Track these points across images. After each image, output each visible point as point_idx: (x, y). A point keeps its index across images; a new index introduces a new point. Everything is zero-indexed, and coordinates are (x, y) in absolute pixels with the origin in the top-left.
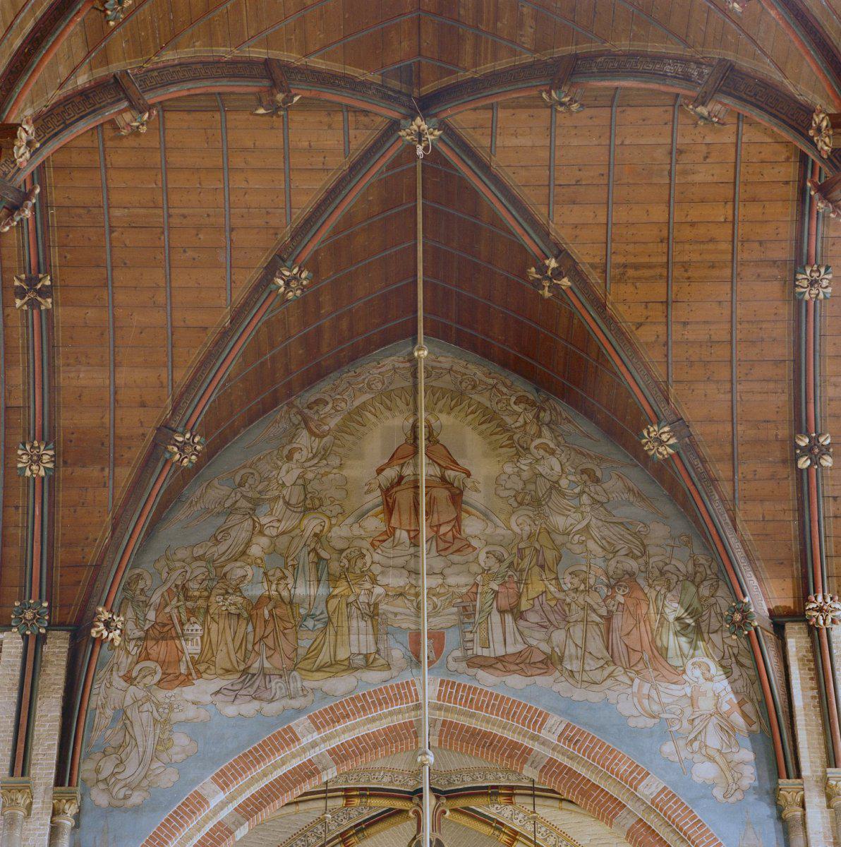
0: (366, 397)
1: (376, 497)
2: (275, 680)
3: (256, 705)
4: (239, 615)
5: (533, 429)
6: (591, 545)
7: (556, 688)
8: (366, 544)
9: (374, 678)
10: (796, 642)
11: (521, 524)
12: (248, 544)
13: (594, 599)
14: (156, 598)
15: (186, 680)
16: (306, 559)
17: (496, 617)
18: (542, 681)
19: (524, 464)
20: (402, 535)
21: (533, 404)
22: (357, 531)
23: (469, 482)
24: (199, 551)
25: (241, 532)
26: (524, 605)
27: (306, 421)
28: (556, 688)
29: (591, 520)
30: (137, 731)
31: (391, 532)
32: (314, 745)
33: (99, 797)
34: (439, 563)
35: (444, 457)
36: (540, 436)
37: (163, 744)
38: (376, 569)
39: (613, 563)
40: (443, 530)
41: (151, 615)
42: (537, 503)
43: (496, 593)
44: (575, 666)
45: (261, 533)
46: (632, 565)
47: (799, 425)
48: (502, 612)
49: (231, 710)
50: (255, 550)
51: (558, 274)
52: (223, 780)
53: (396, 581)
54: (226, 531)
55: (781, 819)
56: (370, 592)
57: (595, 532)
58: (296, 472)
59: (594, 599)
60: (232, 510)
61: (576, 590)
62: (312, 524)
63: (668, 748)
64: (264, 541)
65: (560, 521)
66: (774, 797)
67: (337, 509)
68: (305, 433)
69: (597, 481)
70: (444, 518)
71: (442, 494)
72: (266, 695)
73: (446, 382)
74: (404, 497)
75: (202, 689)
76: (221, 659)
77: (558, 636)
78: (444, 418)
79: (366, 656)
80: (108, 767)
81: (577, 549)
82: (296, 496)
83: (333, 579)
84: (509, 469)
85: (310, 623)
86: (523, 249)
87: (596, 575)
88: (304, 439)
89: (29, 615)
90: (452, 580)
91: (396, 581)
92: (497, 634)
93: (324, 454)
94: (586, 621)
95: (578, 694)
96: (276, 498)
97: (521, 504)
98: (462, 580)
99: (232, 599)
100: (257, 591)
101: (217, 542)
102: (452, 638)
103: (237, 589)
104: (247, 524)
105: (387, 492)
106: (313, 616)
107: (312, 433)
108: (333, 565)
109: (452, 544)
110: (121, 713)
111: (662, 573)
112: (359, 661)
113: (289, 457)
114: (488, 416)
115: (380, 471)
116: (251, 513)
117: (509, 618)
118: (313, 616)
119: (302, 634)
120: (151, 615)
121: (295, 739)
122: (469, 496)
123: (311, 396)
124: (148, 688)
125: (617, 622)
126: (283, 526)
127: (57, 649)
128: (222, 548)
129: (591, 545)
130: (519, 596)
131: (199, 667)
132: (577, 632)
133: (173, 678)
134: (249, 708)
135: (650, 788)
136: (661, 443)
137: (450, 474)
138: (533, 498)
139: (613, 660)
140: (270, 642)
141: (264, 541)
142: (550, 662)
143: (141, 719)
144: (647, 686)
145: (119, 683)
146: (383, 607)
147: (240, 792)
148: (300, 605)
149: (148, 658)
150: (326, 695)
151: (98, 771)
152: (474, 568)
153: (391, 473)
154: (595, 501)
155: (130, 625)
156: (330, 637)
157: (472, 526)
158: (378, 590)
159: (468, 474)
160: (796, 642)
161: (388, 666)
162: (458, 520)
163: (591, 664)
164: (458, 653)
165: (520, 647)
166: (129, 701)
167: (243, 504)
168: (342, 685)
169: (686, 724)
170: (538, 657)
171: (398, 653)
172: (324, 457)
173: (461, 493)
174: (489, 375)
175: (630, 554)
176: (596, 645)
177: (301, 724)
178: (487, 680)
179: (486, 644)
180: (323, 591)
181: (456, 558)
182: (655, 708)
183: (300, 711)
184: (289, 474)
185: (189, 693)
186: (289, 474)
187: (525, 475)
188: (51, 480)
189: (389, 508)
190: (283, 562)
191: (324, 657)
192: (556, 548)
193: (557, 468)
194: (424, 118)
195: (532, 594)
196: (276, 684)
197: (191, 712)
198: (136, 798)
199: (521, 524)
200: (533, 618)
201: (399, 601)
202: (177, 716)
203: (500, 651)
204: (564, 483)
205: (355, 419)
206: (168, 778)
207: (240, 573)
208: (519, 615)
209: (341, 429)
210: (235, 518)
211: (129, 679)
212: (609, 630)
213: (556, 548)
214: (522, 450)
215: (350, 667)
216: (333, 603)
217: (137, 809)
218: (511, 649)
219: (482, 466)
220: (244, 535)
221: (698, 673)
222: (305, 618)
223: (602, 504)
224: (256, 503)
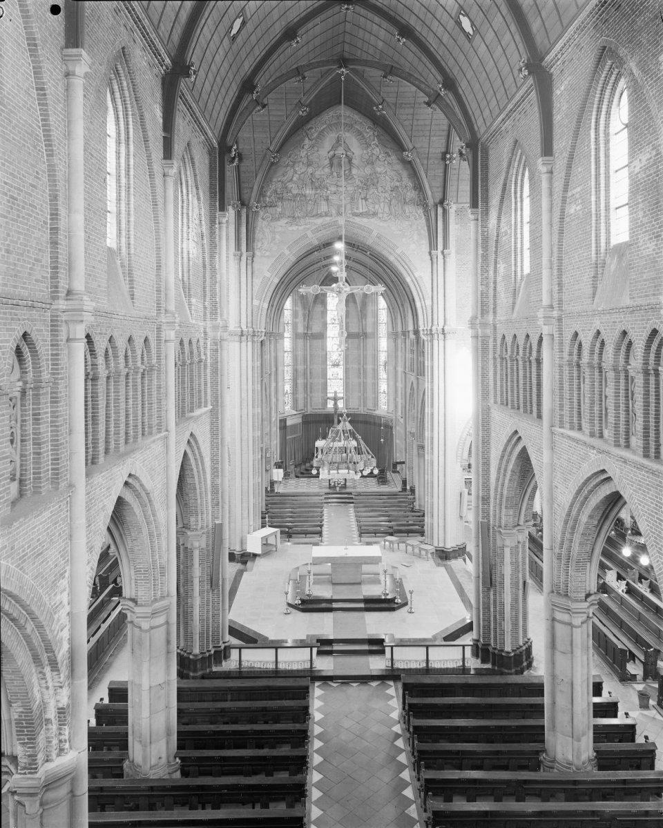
1: (327, 162)
9: (328, 219)
10: (440, 210)
11: (368, 170)
15: (278, 219)
16: (309, 181)
17: (360, 201)
18: (372, 220)
20: (335, 174)
22: (322, 173)
25: (290, 173)
29: (388, 170)
31: (332, 174)
33: (258, 253)
35: (347, 149)
37: (273, 239)
38: (328, 185)
41: (268, 199)
42: (372, 163)
46: (398, 184)
47: (447, 152)
49: (290, 229)
50: (295, 179)
51: (382, 109)
53: (333, 189)
55: (431, 259)
58: (305, 153)
59: (387, 195)
60: (288, 165)
62: (310, 170)
63: (404, 240)
64: (297, 176)
65: (379, 170)
66: (430, 253)
74: (335, 161)
75: (283, 222)
76: (287, 213)
77: (377, 207)
82: (305, 160)
83: (316, 188)
86: (372, 101)
87: (388, 188)
88: (307, 141)
91: (333, 189)
92: (360, 206)
93: (312, 147)
95: (381, 224)
100: (295, 192)
102: (349, 207)
105: (331, 159)
107: (309, 139)
108: (317, 184)
109: (349, 177)
114: (360, 133)
116: (293, 166)
122: (354, 161)
123: (309, 126)
127: (244, 211)
131: (281, 216)
132: (382, 205)
133: (274, 219)
134: (295, 228)
135: (398, 251)
137: (349, 153)
141: (297, 176)
142: (375, 214)
143: (267, 231)
146: (330, 197)
153: (332, 153)
154: (388, 163)
157: (354, 171)
160: (440, 210)
162: (350, 169)
167: (291, 163)
168: (319, 221)
170: (371, 213)
171: (334, 212)
176: (387, 209)
177: (309, 234)
178: (357, 220)
179: (357, 209)
184: (303, 153)
185: (279, 223)
189: (331, 165)
191: (314, 213)
194: (346, 67)
197: (280, 229)
198: (267, 254)
200: (370, 200)
203: (361, 211)
205: (321, 135)
208: (366, 199)
209: (318, 137)
210: (289, 168)
214: (368, 145)
215: (321, 216)
219: (356, 149)
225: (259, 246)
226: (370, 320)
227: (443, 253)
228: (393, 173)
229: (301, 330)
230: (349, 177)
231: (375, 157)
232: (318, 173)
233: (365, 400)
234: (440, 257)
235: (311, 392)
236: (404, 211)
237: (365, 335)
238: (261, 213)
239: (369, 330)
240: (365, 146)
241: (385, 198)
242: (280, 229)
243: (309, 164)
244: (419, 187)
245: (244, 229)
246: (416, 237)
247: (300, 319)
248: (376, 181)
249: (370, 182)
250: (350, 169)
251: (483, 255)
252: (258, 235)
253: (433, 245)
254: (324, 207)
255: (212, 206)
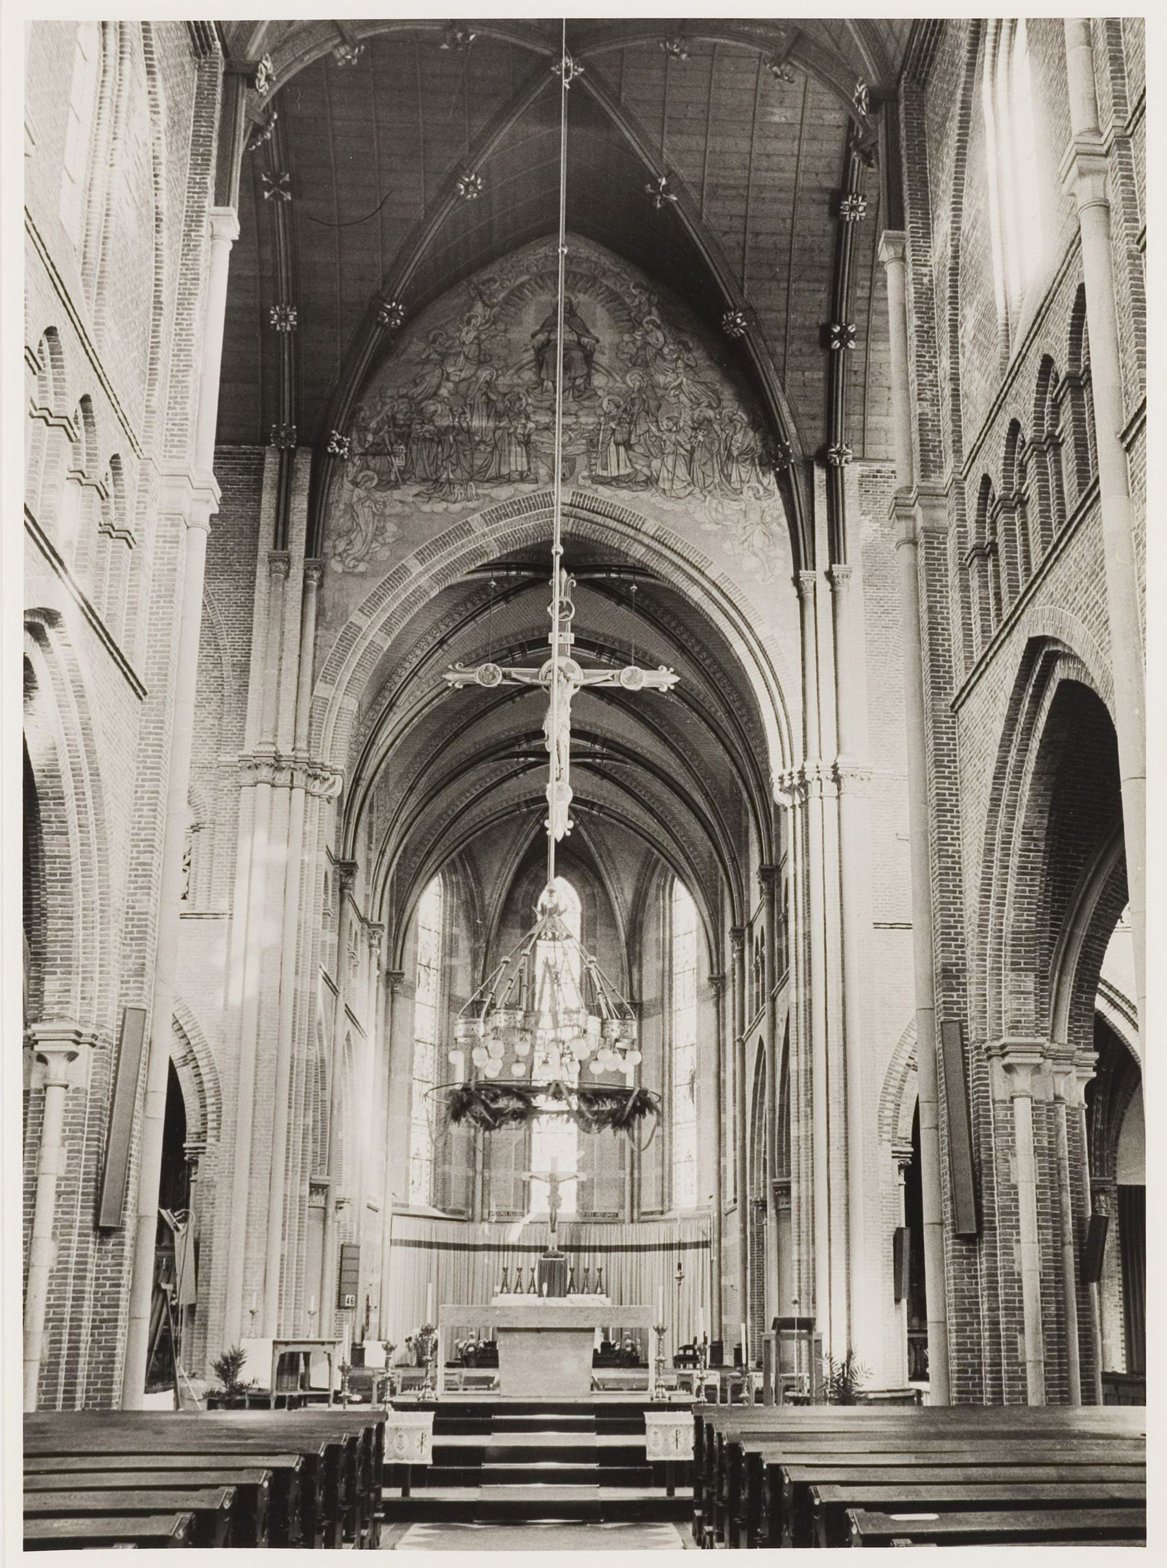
0: (525, 278)
1: (529, 355)
2: (457, 487)
3: (444, 505)
4: (432, 440)
5: (645, 309)
6: (683, 398)
7: (653, 500)
8: (522, 390)
9: (527, 488)
10: (820, 475)
11: (633, 380)
12: (439, 387)
13: (681, 438)
14: (373, 425)
15: (396, 486)
17: (613, 448)
19: (638, 335)
21: (646, 289)
23: (597, 346)
24: (403, 391)
25: (433, 379)
26: (633, 440)
27: (480, 295)
28: (653, 500)
30: (361, 520)
32: (484, 535)
33: (336, 566)
34: (574, 407)
36: (650, 313)
37: (380, 531)
38: (530, 409)
39: (697, 412)
40: (579, 382)
41: (370, 438)
42: (646, 365)
43: (614, 430)
44: (667, 486)
45: (448, 379)
46: (710, 413)
48: (617, 444)
49: (426, 508)
50: (444, 392)
52: (421, 557)
53: (544, 419)
54: (423, 376)
56: (525, 426)
57: (685, 388)
58: (473, 334)
59: (681, 438)
60: (427, 361)
61: (670, 430)
62: (485, 374)
63: (727, 546)
64: (450, 385)
65: (661, 379)
66: (797, 581)
67: (502, 364)
68: (480, 304)
69: (689, 350)
70: (580, 373)
71: (577, 354)
72: (452, 498)
73: (583, 269)
76: (419, 471)
77: (656, 463)
78: (582, 297)
79: (521, 473)
80: (342, 545)
81: (673, 400)
82: (472, 351)
84: (626, 337)
85: (482, 447)
87: (685, 420)
88: (479, 308)
89: (283, 434)
90: (582, 420)
94: (675, 453)
95: (668, 506)
96: (458, 354)
97: (634, 365)
98: (591, 420)
99: (427, 427)
100: (445, 422)
101: (416, 385)
102: (581, 462)
103: (431, 421)
104: (438, 372)
106: (484, 442)
107: (485, 305)
109: (581, 393)
110: (350, 506)
111: (731, 421)
112: (516, 476)
113: (469, 323)
114: (614, 299)
115: (533, 336)
116: (441, 363)
117: (622, 449)
118: (484, 442)
119: (477, 455)
120: (370, 438)
121: (471, 531)
122: (597, 357)
123: (486, 275)
124: (368, 490)
125: (697, 455)
126: (463, 375)
128: (420, 389)
129: (683, 398)
130: (630, 433)
131: (405, 477)
132: (669, 461)
133: (386, 484)
134: (440, 507)
136: (736, 325)
137: (585, 340)
138: (641, 361)
139: (692, 483)
140: (454, 460)
141: (450, 385)
142: (650, 482)
143: (364, 514)
144: (715, 502)
145: (348, 485)
146: (533, 438)
147: (433, 566)
148: (475, 434)
149: (368, 468)
150: (492, 500)
151: (334, 547)
152: (599, 412)
153: (541, 337)
154: (687, 365)
155: (355, 443)
156: (496, 458)
157: (599, 380)
158: (531, 425)
159: (598, 341)
160: (820, 475)
161: (536, 481)
163: (678, 485)
164: (585, 473)
165: (629, 470)
166: (355, 499)
167: (434, 356)
168: (503, 493)
169: (740, 530)
171: (543, 472)
172: (494, 323)
173: (592, 355)
174: (616, 264)
175: (710, 406)
176: (682, 471)
177: (475, 519)
178: (604, 492)
179: (605, 468)
180: (491, 424)
181: (586, 403)
182: (720, 517)
183: (474, 510)
184: (468, 335)
185: (397, 494)
186: (468, 335)
187: (639, 344)
188: (295, 334)
190: (463, 401)
191: (492, 472)
192: (657, 399)
193: (662, 339)
195: (639, 432)
196: (458, 490)
197: (398, 508)
198: (362, 567)
199: (633, 380)
200: (639, 449)
201: (545, 433)
202: (388, 511)
203: (615, 474)
204: (666, 350)
205: (516, 296)
206: (384, 554)
207: (432, 408)
208: (628, 446)
209: (506, 301)
210: (428, 368)
211: (355, 484)
212: (691, 460)
213: (657, 399)
215: (509, 480)
216: (499, 432)
217: (362, 575)
218: (623, 472)
219: (604, 333)
220: (435, 381)
221: (751, 493)
222: (478, 443)
223: (692, 368)
224: (444, 356)
225: (340, 549)
226: (651, 966)
227: (829, 575)
228: (697, 390)
229: (463, 989)
230: (581, 393)
231: (650, 352)
232: (503, 382)
233: (636, 1185)
234: (824, 586)
235: (486, 1165)
236: (728, 478)
237: (638, 1007)
238: (351, 470)
239: (649, 994)
240: (629, 324)
241: (678, 444)
242: (398, 508)
243: (483, 360)
244: (764, 420)
245: (300, 504)
246: (758, 540)
247: (462, 960)
248: (653, 404)
249: (640, 407)
250: (589, 376)
251: (920, 330)
252: (338, 518)
253: (801, 557)
254: (517, 461)
255: (195, 187)
